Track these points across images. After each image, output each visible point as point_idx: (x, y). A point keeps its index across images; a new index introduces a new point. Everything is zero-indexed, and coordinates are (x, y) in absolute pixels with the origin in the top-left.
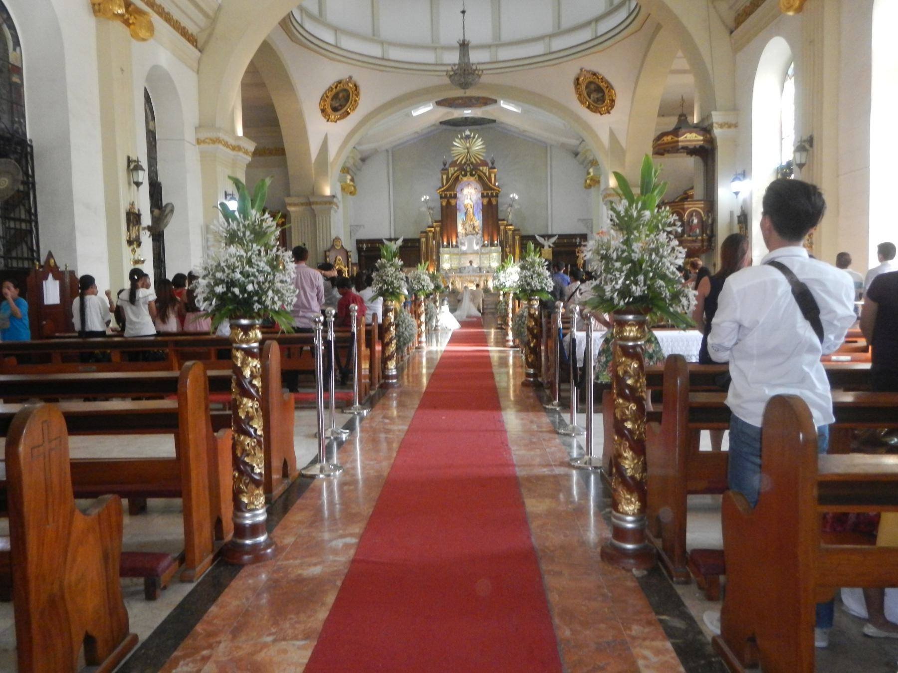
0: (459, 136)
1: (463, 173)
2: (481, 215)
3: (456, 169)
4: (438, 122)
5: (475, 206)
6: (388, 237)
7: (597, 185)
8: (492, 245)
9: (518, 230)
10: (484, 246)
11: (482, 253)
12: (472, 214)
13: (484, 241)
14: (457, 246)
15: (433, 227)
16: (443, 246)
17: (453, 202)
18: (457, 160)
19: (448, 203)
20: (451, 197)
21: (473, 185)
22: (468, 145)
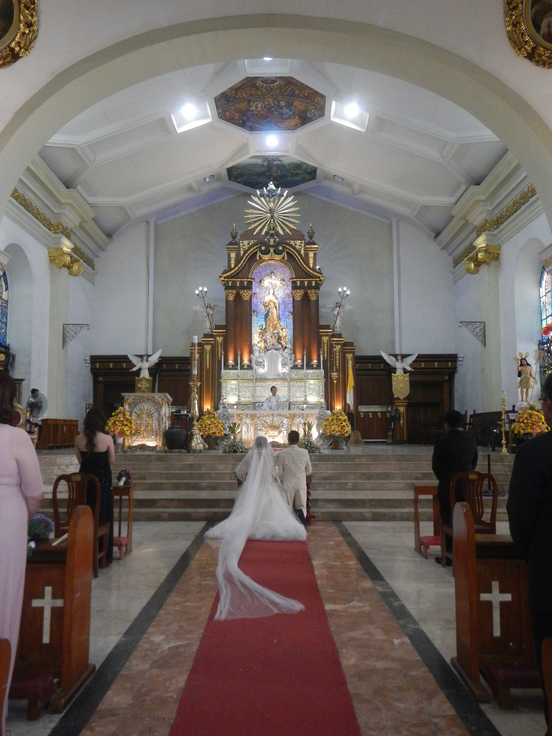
0: (258, 193)
1: (263, 248)
2: (290, 321)
3: (252, 242)
4: (225, 173)
5: (282, 306)
6: (142, 353)
7: (493, 263)
8: (310, 366)
9: (351, 344)
10: (295, 367)
11: (292, 380)
12: (276, 318)
13: (295, 361)
14: (250, 367)
15: (211, 336)
16: (227, 367)
17: (246, 295)
18: (254, 230)
19: (238, 297)
20: (243, 287)
21: (278, 274)
22: (272, 205)
